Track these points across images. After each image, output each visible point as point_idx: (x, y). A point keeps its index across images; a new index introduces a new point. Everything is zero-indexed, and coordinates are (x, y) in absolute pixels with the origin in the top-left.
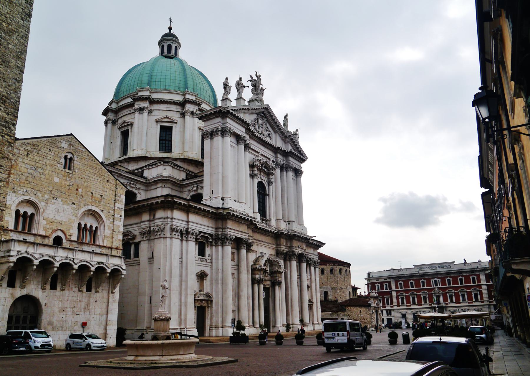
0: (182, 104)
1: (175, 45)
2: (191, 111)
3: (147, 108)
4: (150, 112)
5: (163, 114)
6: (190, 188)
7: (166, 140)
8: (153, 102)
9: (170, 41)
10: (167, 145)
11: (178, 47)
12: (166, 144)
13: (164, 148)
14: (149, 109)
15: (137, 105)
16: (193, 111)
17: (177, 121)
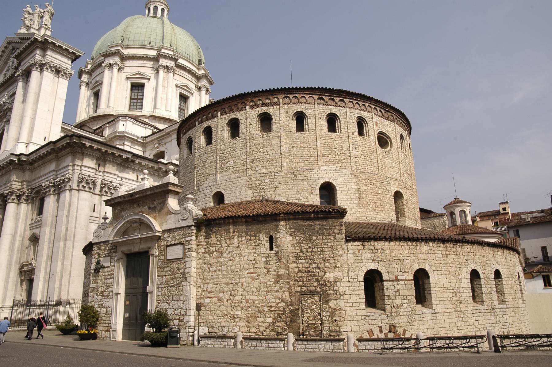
0: (156, 59)
1: (162, 7)
2: (165, 65)
3: (116, 64)
4: (120, 69)
5: (135, 70)
6: (152, 146)
7: (137, 99)
8: (124, 58)
9: (156, 3)
10: (139, 104)
11: (165, 8)
12: (137, 102)
13: (135, 107)
14: (120, 65)
15: (108, 61)
16: (167, 66)
17: (150, 77)
